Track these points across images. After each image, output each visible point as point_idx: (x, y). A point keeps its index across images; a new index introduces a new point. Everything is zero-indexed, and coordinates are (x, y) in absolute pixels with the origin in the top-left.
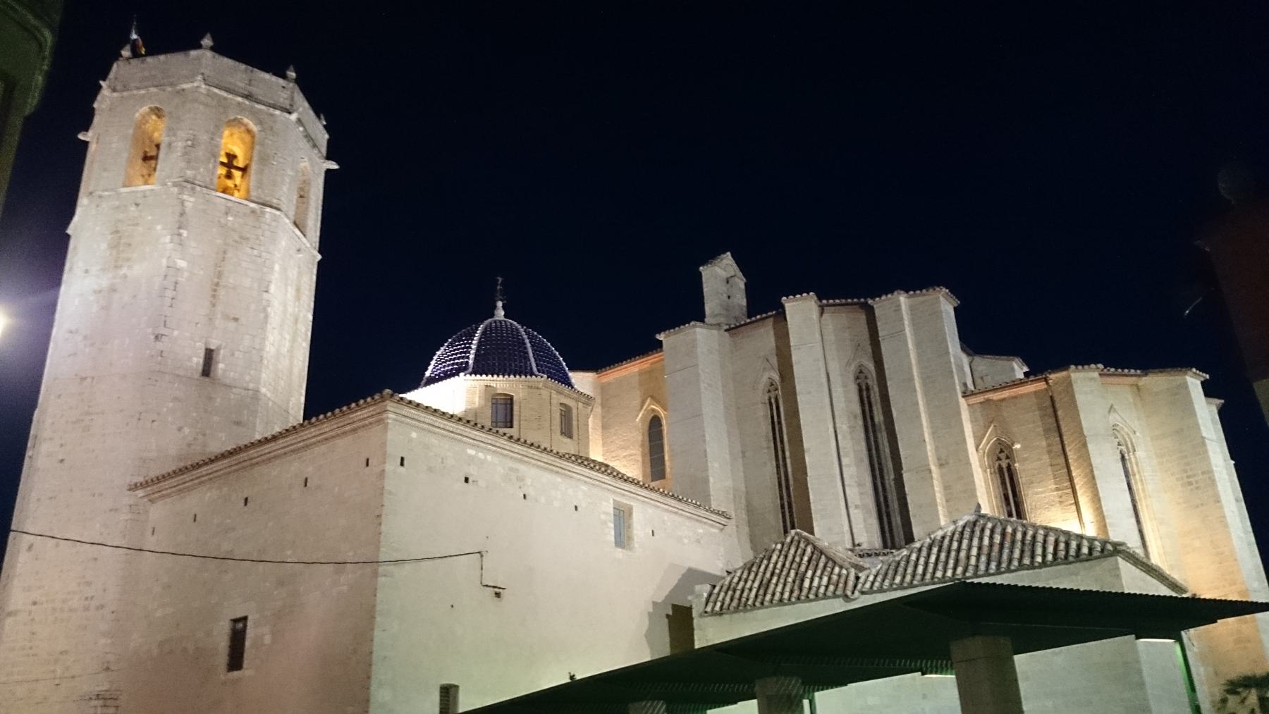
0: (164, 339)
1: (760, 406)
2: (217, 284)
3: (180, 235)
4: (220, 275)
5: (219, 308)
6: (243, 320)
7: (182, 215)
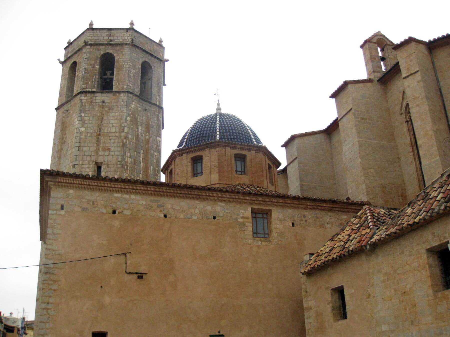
0: (76, 166)
1: (405, 124)
2: (99, 135)
3: (81, 116)
4: (100, 130)
5: (101, 145)
6: (112, 149)
7: (81, 106)
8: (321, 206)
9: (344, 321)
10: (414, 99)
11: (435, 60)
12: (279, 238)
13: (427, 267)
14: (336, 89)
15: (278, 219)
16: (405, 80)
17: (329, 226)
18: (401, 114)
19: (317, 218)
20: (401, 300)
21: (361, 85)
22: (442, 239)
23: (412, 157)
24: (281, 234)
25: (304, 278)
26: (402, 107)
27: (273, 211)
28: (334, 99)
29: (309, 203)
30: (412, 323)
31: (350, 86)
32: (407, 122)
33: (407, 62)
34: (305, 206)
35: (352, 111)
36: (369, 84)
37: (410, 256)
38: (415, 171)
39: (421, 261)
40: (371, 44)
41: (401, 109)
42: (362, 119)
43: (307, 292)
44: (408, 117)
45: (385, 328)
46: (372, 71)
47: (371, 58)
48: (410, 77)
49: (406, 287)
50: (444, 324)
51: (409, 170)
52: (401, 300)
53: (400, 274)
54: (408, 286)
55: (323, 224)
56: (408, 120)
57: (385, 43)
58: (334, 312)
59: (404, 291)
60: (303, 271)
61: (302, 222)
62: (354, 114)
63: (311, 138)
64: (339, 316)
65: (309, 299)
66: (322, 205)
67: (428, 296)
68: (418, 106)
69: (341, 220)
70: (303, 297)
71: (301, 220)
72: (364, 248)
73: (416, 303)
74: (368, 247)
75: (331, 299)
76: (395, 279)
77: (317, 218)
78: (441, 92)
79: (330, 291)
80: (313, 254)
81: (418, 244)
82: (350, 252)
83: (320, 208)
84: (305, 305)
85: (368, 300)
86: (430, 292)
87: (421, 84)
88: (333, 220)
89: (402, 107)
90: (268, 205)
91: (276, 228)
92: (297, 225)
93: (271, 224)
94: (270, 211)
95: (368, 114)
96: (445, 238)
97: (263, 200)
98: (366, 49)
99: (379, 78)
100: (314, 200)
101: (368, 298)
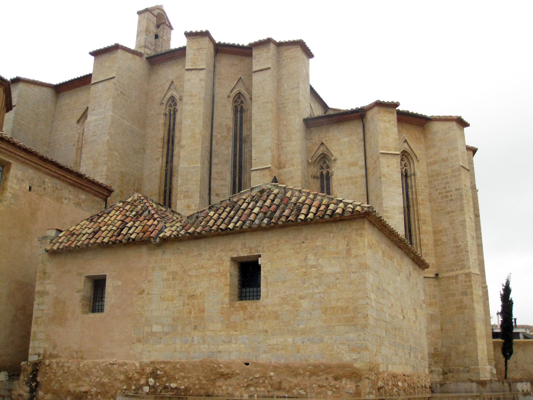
1: (162, 117)
8: (65, 177)
9: (97, 315)
10: (191, 96)
11: (217, 65)
12: (12, 200)
13: (228, 275)
14: (102, 48)
15: (16, 176)
16: (187, 72)
17: (65, 202)
18: (162, 104)
19: (57, 189)
20: (186, 302)
21: (130, 55)
22: (253, 251)
23: (160, 154)
24: (15, 196)
25: (46, 255)
26: (165, 96)
27: (12, 165)
28: (93, 57)
29: (54, 169)
30: (195, 328)
31: (120, 51)
32: (166, 115)
33: (195, 55)
34: (48, 171)
35: (114, 80)
36: (138, 58)
37: (209, 260)
38: (159, 169)
39: (221, 267)
40: (151, 15)
41: (163, 99)
42: (121, 92)
43: (45, 273)
44: (168, 110)
45: (156, 328)
46: (143, 44)
47: (147, 31)
48: (193, 72)
49: (195, 291)
50: (236, 333)
51: (155, 166)
52: (186, 302)
53: (192, 276)
54: (199, 291)
55: (61, 198)
56: (167, 113)
57: (164, 21)
58: (83, 302)
59: (192, 294)
60: (48, 248)
61: (40, 189)
62: (115, 84)
63: (37, 89)
64: (88, 308)
65: (48, 281)
66: (66, 176)
67: (222, 304)
68: (193, 104)
69: (79, 199)
70: (37, 278)
71: (40, 186)
72: (152, 240)
73: (205, 308)
74: (158, 240)
75: (82, 287)
76: (182, 279)
77: (57, 189)
78: (213, 99)
79: (83, 279)
80: (61, 231)
81: (222, 250)
82: (131, 240)
83: (62, 178)
84: (38, 288)
85: (139, 296)
86: (227, 300)
87: (203, 84)
88: (71, 197)
89: (165, 96)
90: (9, 156)
91: (11, 187)
92: (34, 191)
93: (5, 180)
94: (9, 164)
95: (128, 90)
96: (257, 251)
97: (8, 148)
98: (144, 18)
99: (149, 56)
100: (61, 167)
101: (141, 294)
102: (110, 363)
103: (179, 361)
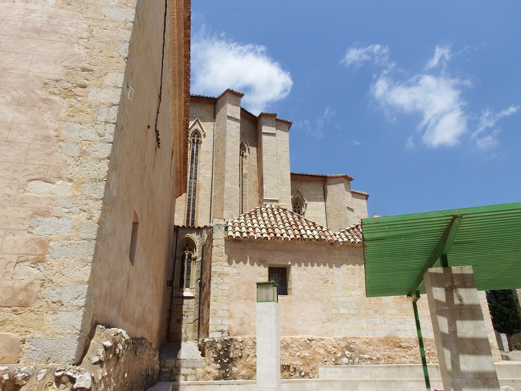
30: (376, 312)
45: (342, 311)
102: (308, 339)
103: (367, 337)
